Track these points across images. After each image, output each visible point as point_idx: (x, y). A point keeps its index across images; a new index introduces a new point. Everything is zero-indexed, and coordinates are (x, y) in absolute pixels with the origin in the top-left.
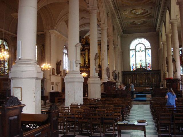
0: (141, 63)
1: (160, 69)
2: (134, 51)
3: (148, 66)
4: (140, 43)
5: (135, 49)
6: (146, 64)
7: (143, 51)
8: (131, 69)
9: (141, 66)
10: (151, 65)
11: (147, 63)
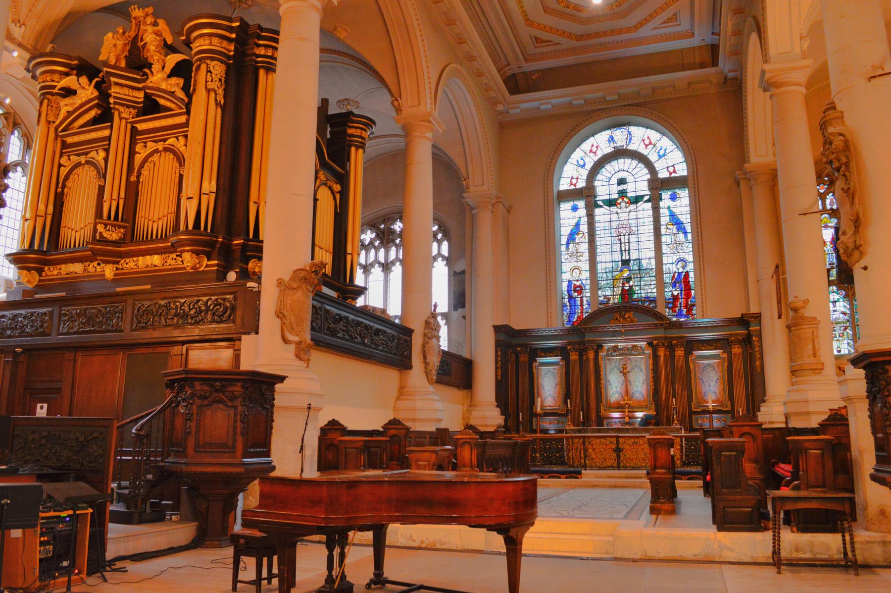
0: (626, 275)
1: (754, 310)
2: (581, 204)
3: (675, 298)
4: (619, 153)
5: (587, 194)
6: (661, 284)
7: (637, 200)
8: (566, 319)
9: (626, 294)
10: (692, 284)
11: (667, 279)
